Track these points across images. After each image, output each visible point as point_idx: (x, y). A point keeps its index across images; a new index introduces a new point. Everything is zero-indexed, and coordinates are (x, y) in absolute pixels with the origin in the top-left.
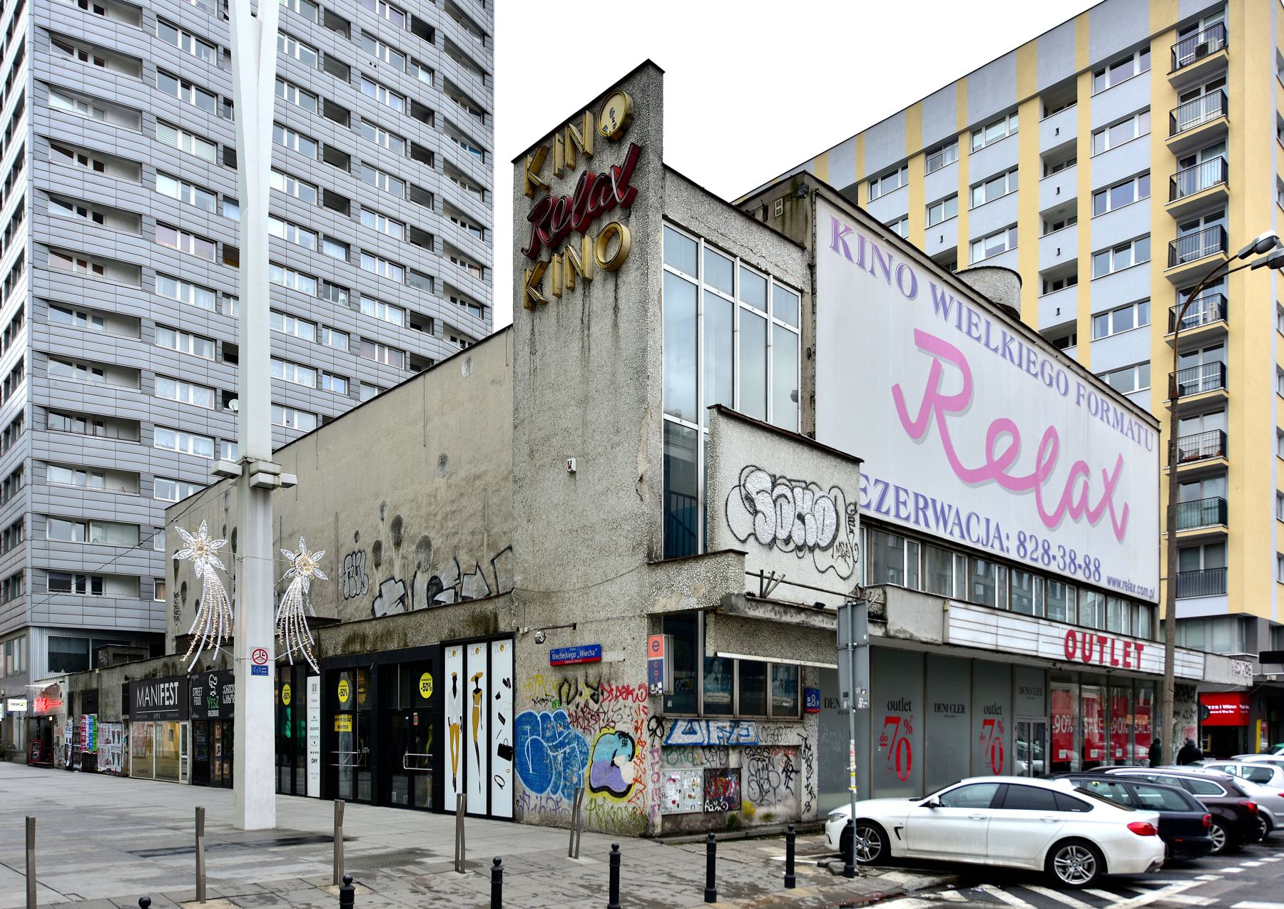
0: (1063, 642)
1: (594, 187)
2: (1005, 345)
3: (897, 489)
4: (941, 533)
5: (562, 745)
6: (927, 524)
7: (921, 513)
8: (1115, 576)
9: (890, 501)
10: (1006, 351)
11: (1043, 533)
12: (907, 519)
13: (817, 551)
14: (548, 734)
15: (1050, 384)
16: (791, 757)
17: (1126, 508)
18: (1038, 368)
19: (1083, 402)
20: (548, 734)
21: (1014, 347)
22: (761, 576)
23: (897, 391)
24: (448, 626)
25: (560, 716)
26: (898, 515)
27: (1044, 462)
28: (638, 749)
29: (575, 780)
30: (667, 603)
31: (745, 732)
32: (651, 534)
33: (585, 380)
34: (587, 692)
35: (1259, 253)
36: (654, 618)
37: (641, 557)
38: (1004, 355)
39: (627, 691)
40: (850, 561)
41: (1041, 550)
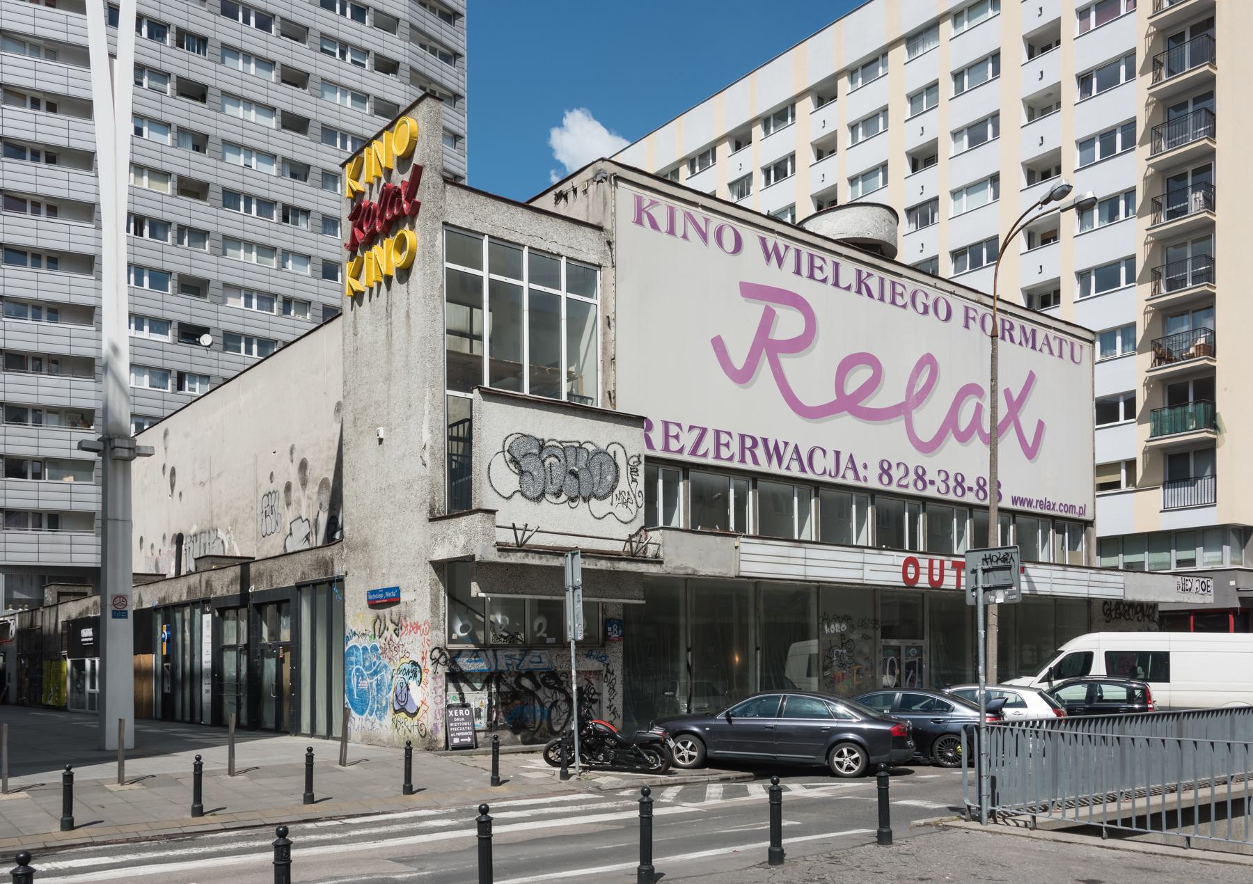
0: (901, 569)
1: (390, 196)
2: (860, 281)
3: (717, 433)
4: (774, 469)
5: (375, 673)
6: (755, 461)
7: (748, 454)
8: (1022, 495)
9: (708, 443)
10: (861, 286)
11: (914, 458)
12: (731, 459)
13: (593, 501)
14: (367, 664)
15: (926, 312)
16: (593, 681)
17: (1041, 425)
18: (907, 298)
19: (975, 326)
20: (367, 664)
21: (874, 284)
22: (514, 527)
23: (718, 343)
24: (301, 569)
25: (375, 648)
26: (718, 456)
27: (918, 389)
28: (424, 675)
29: (384, 703)
30: (441, 554)
31: (537, 659)
32: (432, 493)
33: (389, 361)
34: (392, 627)
35: (1057, 200)
36: (433, 563)
37: (425, 514)
38: (859, 292)
39: (417, 627)
40: (633, 507)
41: (912, 476)
